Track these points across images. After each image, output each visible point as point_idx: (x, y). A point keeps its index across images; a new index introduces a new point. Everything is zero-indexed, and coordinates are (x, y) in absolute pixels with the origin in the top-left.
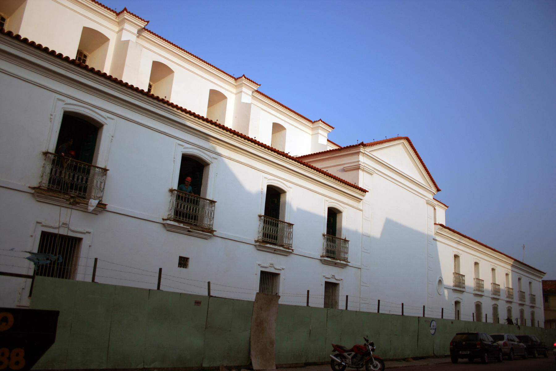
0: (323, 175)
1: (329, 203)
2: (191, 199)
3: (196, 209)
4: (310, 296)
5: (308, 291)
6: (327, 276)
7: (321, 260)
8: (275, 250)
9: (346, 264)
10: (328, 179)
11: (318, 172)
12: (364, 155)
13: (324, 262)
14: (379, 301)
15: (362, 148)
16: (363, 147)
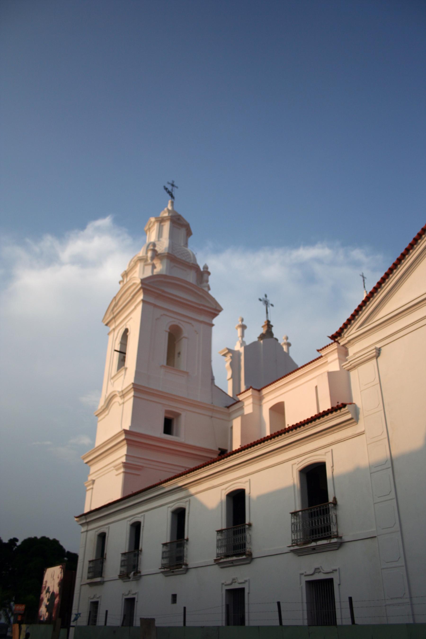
0: (269, 441)
1: (298, 464)
2: (314, 512)
3: (327, 518)
4: (187, 613)
5: (185, 608)
6: (308, 573)
7: (292, 551)
8: (232, 562)
9: (328, 542)
10: (285, 437)
11: (262, 444)
12: (352, 342)
13: (298, 553)
14: (279, 603)
15: (340, 339)
16: (339, 338)
